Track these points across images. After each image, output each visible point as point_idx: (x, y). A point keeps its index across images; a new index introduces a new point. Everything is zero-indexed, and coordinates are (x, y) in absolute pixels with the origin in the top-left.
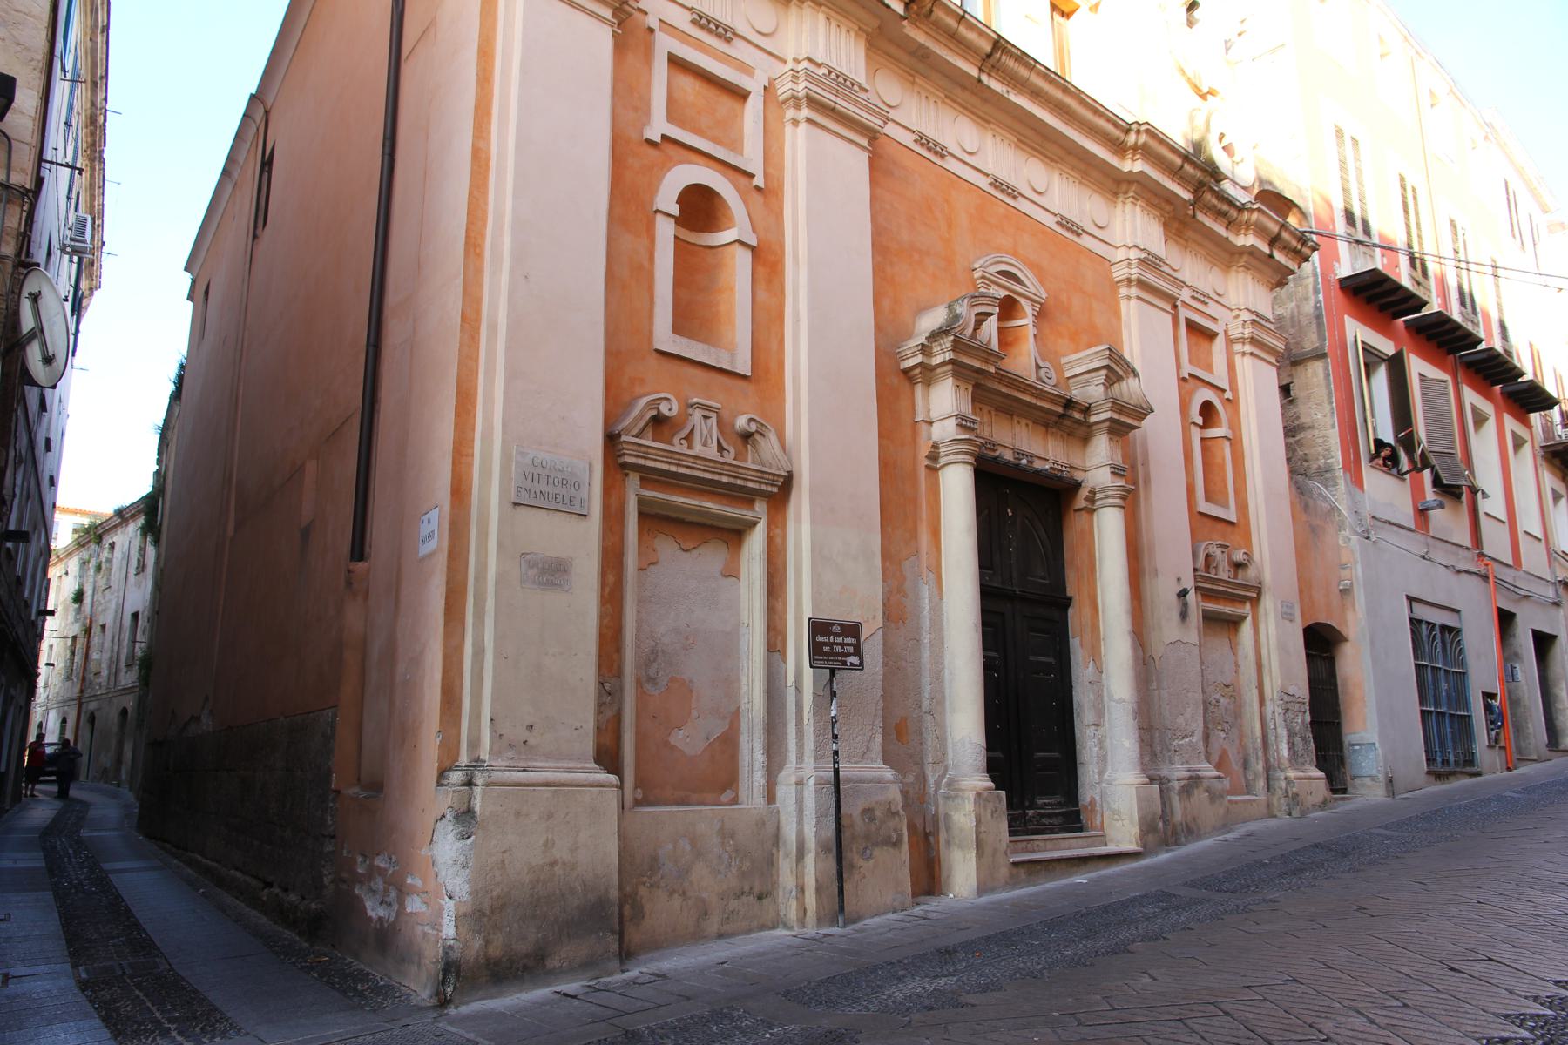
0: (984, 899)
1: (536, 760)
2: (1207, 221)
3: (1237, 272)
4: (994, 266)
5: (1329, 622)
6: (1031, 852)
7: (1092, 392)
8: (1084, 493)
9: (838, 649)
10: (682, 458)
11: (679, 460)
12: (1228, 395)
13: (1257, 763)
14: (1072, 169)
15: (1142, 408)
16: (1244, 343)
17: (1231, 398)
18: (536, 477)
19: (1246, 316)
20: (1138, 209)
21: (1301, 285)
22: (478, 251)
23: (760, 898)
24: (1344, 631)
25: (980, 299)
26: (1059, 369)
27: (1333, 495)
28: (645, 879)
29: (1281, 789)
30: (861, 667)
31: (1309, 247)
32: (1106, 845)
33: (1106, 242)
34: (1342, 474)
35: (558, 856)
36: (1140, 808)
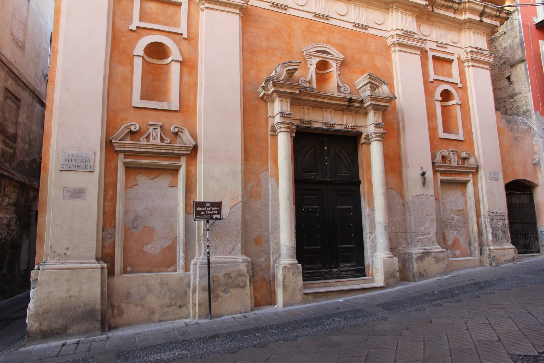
0: (287, 308)
1: (69, 260)
2: (442, 12)
3: (466, 31)
4: (313, 49)
5: (525, 179)
6: (328, 287)
7: (366, 93)
8: (363, 136)
9: (209, 212)
10: (141, 145)
11: (140, 146)
12: (460, 85)
13: (475, 243)
14: (362, 3)
15: (390, 97)
16: (468, 62)
17: (461, 86)
18: (70, 160)
19: (469, 50)
20: (399, 13)
21: (513, 31)
22: (53, 83)
23: (180, 307)
24: (535, 182)
25: (289, 64)
26: (352, 86)
27: (530, 122)
28: (124, 300)
29: (487, 254)
30: (221, 218)
31: (504, 13)
32: (374, 282)
33: (383, 30)
34: (534, 112)
35: (73, 294)
36: (385, 268)
